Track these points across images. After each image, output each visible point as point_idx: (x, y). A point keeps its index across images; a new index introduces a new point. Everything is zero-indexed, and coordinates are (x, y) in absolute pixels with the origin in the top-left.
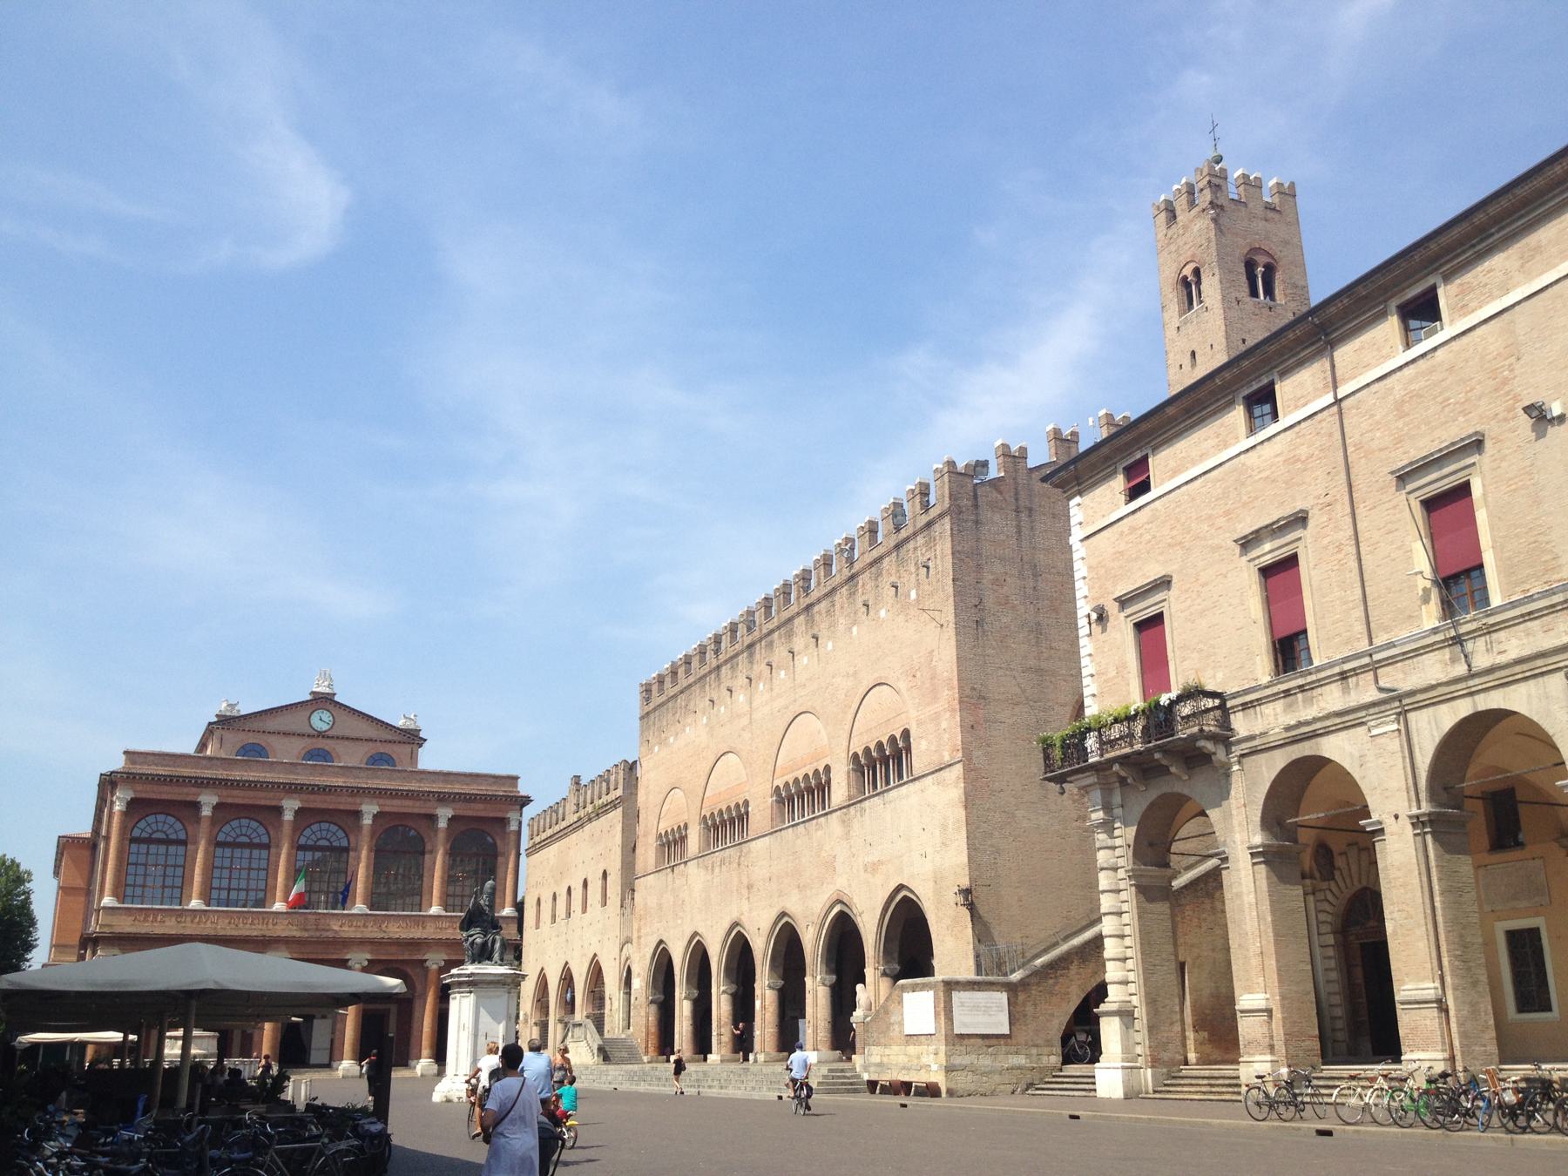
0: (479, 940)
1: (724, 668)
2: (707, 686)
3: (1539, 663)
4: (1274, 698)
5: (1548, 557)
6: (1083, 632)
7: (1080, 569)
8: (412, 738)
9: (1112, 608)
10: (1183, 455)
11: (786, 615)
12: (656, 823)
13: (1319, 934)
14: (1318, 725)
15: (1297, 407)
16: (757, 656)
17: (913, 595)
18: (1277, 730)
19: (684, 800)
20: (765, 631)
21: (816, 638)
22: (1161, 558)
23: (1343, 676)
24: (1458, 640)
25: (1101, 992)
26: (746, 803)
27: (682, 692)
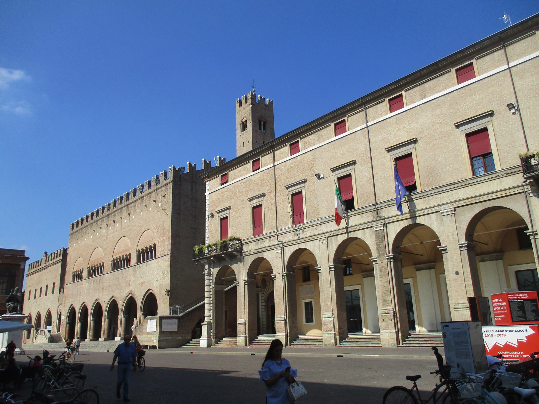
1: (99, 221)
2: (93, 227)
3: (313, 237)
4: (253, 241)
5: (318, 212)
6: (207, 220)
7: (207, 203)
9: (215, 214)
10: (236, 174)
11: (120, 206)
12: (73, 268)
13: (261, 303)
14: (263, 249)
15: (265, 166)
16: (110, 218)
17: (160, 204)
18: (253, 250)
19: (83, 261)
20: (113, 211)
21: (129, 214)
22: (229, 201)
23: (270, 237)
24: (296, 230)
25: (203, 319)
27: (84, 228)
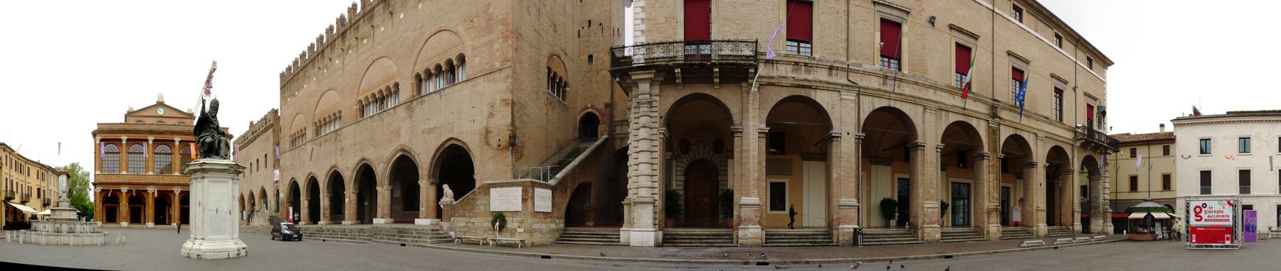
20: (353, 22)
26: (340, 112)
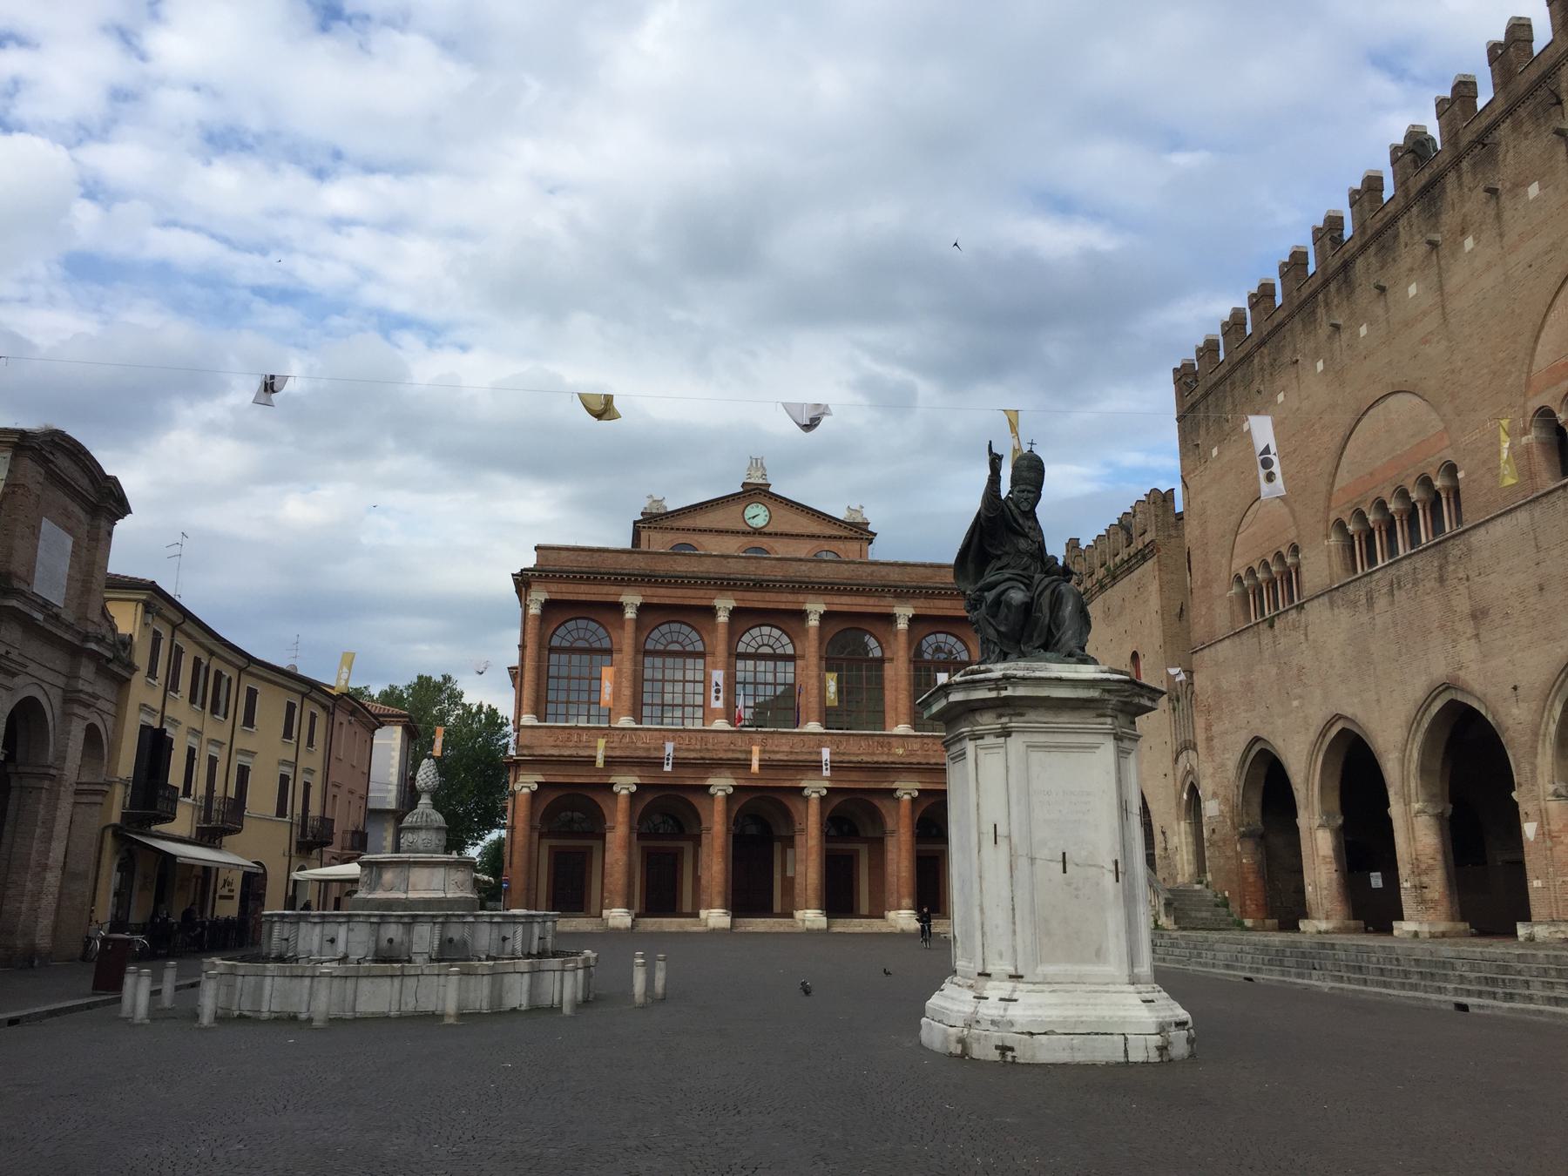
0: (1017, 596)
1: (1358, 261)
8: (860, 532)
12: (1224, 562)
26: (1451, 469)
